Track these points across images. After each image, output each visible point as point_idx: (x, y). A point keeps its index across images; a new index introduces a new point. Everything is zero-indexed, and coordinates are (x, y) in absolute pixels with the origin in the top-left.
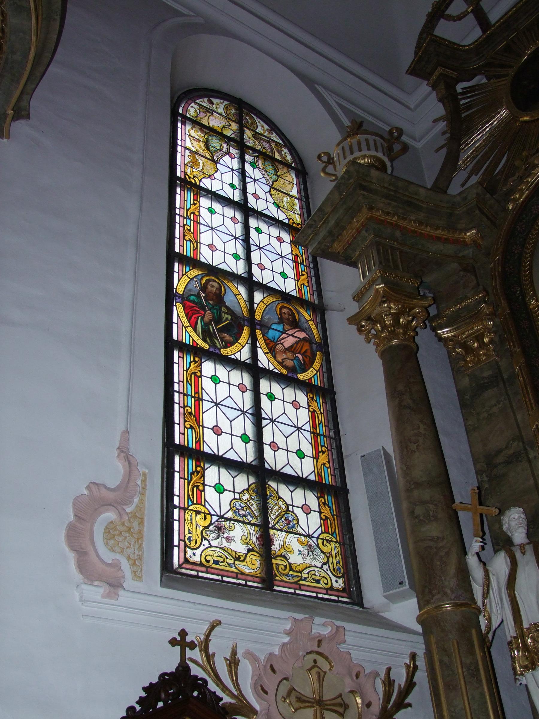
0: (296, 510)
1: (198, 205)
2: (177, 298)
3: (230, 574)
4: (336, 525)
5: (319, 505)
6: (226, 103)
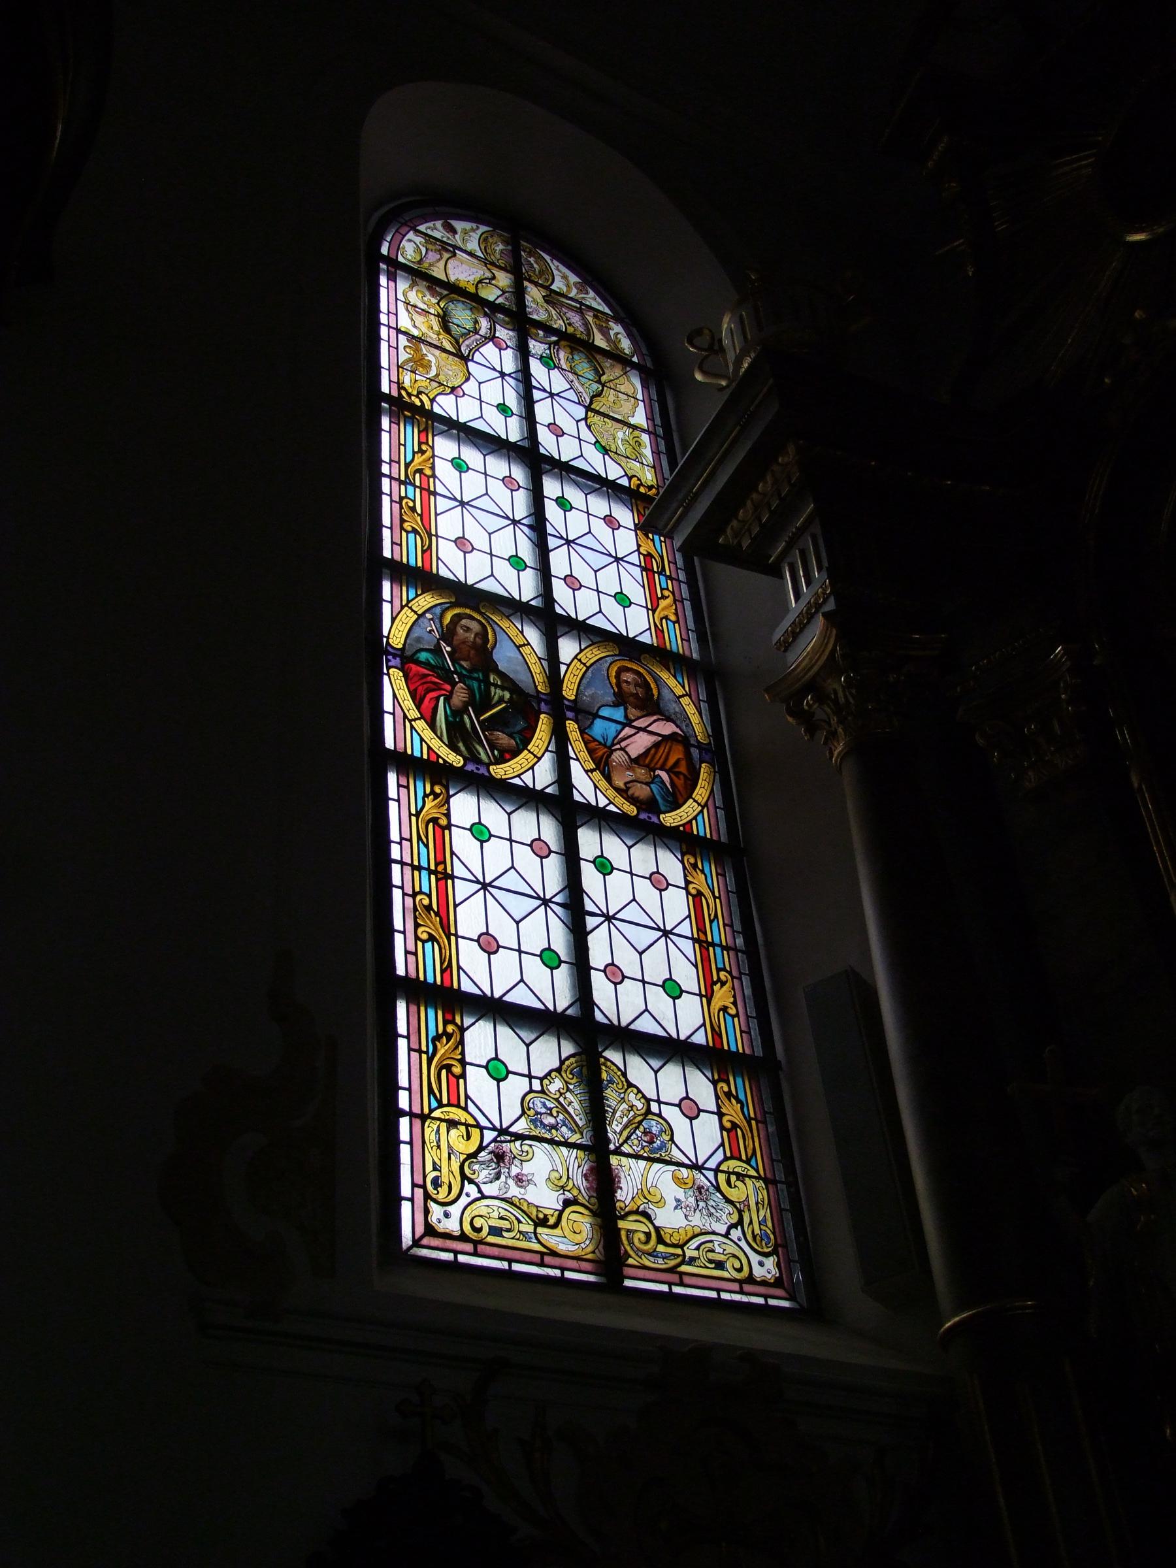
0: (667, 1111)
1: (429, 454)
2: (390, 657)
3: (527, 1256)
4: (756, 1139)
5: (717, 1097)
6: (483, 228)
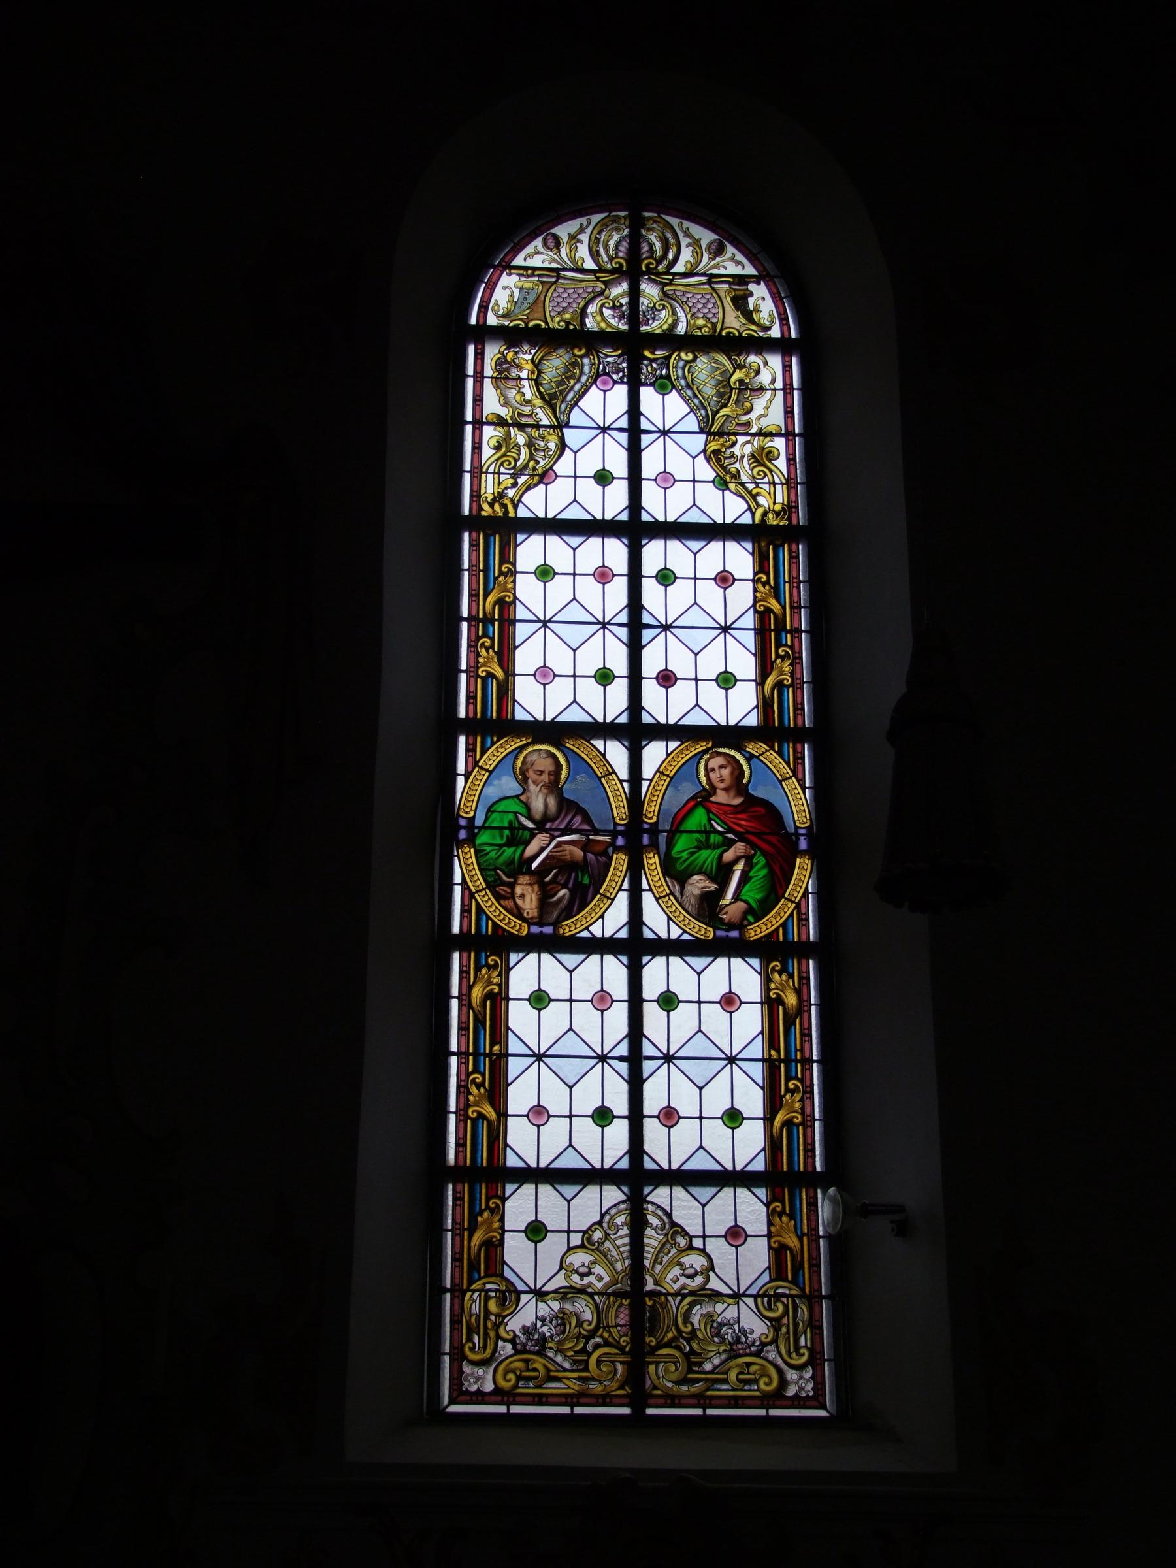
0: (712, 1246)
6: (596, 218)
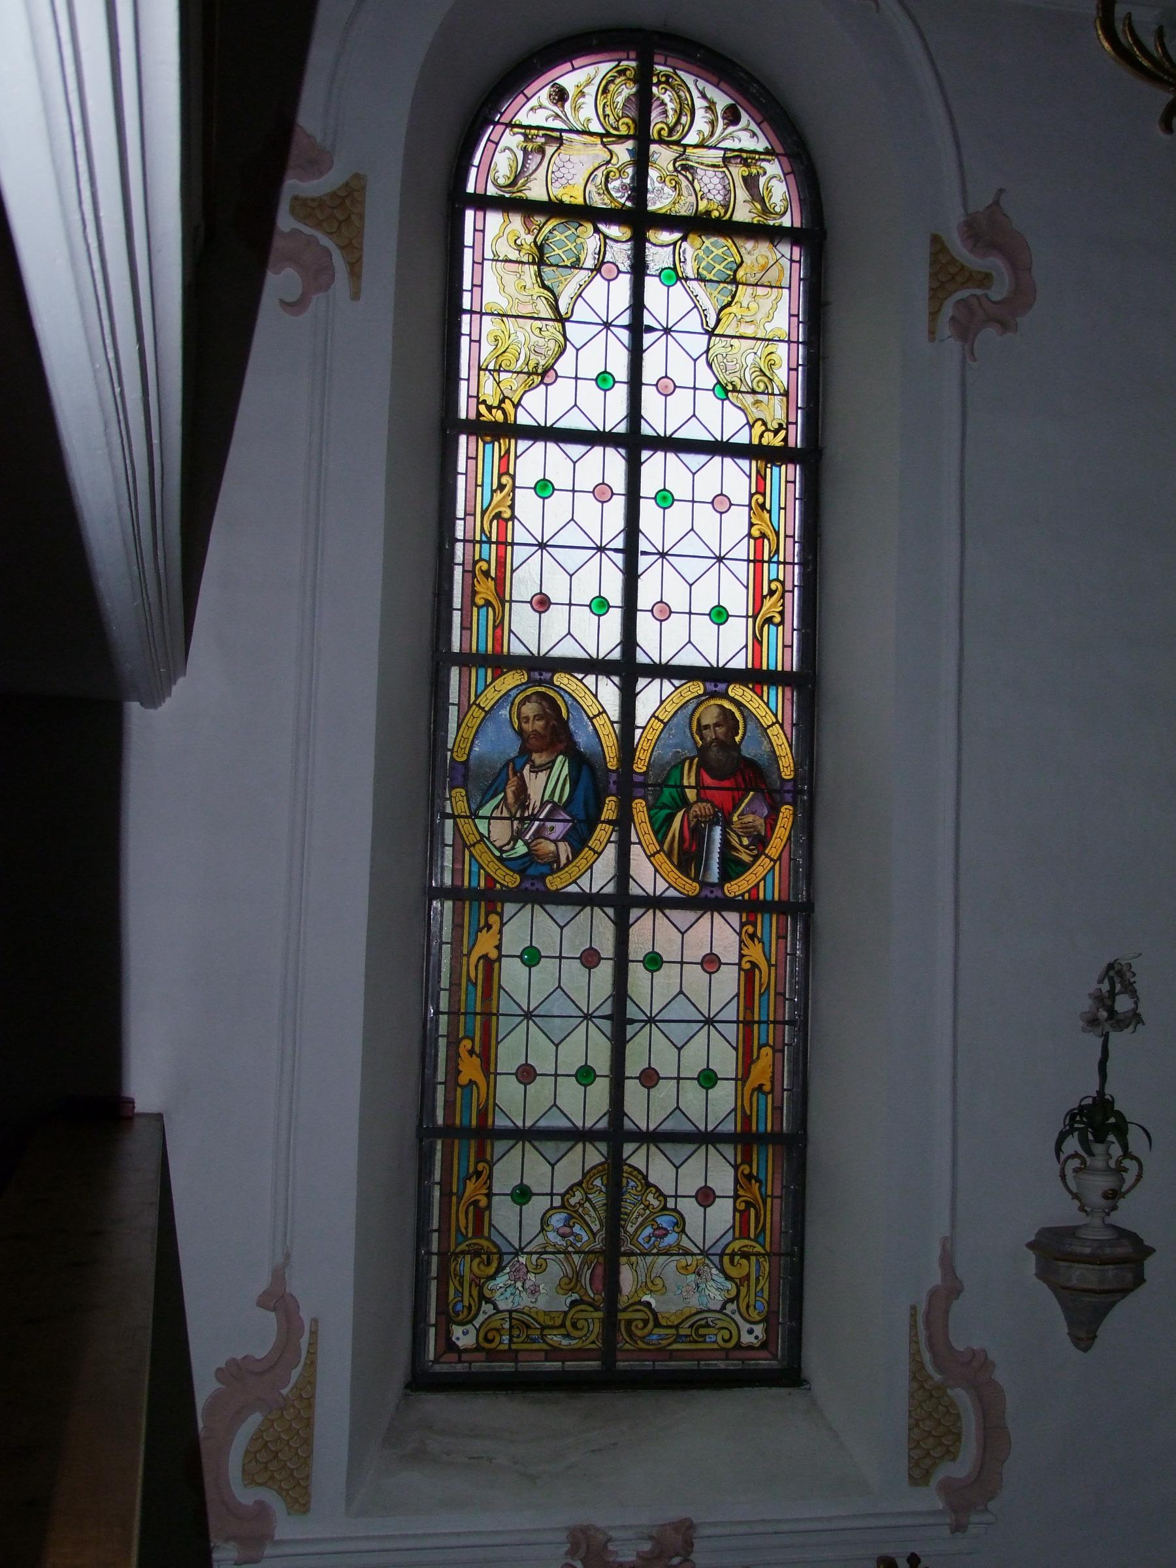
5: (736, 1181)
6: (605, 67)
